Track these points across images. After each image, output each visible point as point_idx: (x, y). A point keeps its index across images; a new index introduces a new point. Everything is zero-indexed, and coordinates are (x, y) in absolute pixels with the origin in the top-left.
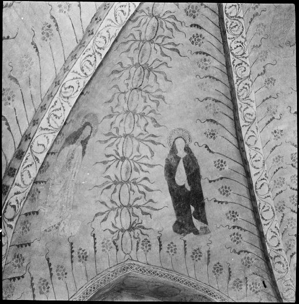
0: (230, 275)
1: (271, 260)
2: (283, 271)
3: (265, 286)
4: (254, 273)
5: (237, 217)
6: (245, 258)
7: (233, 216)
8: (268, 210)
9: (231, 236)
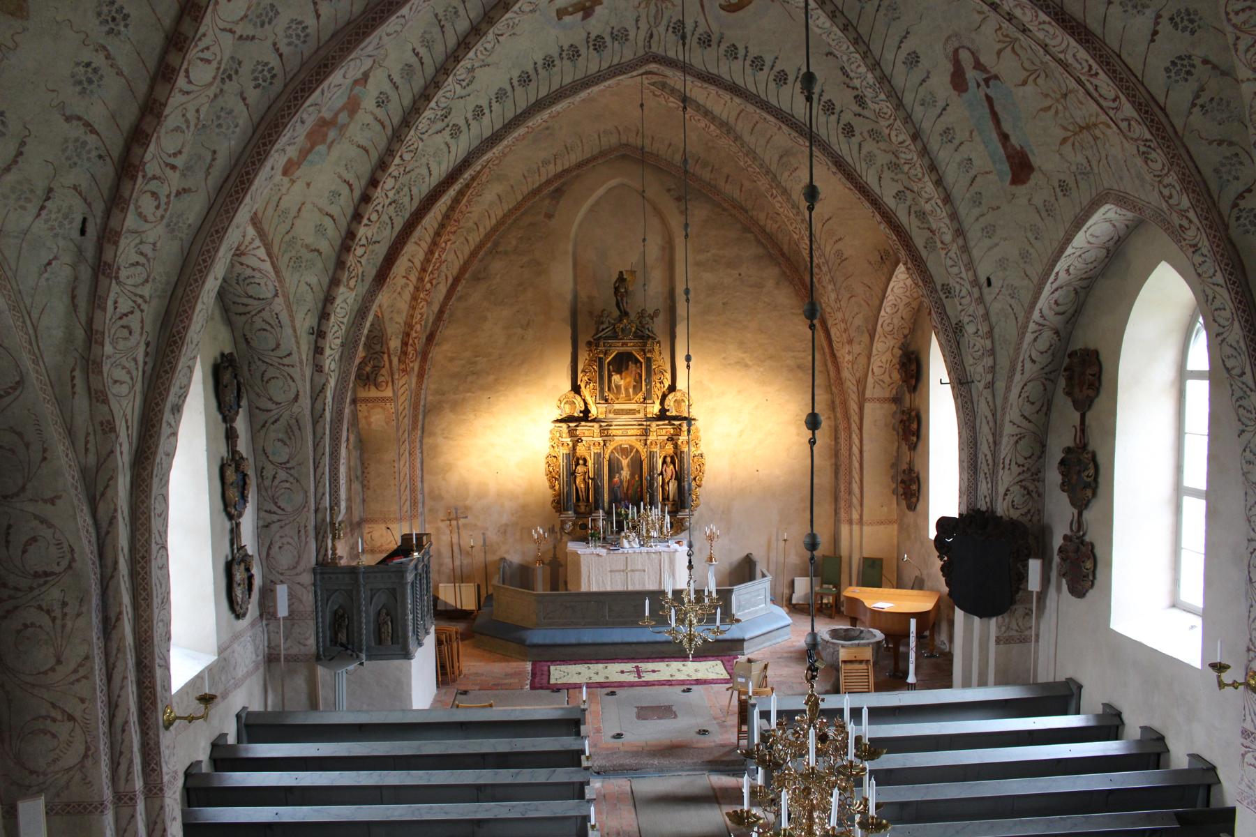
0: (15, 162)
1: (140, 180)
2: (151, 218)
3: (83, 232)
4: (75, 188)
5: (123, 29)
6: (77, 140)
7: (114, 19)
8: (209, 61)
9: (78, 64)
